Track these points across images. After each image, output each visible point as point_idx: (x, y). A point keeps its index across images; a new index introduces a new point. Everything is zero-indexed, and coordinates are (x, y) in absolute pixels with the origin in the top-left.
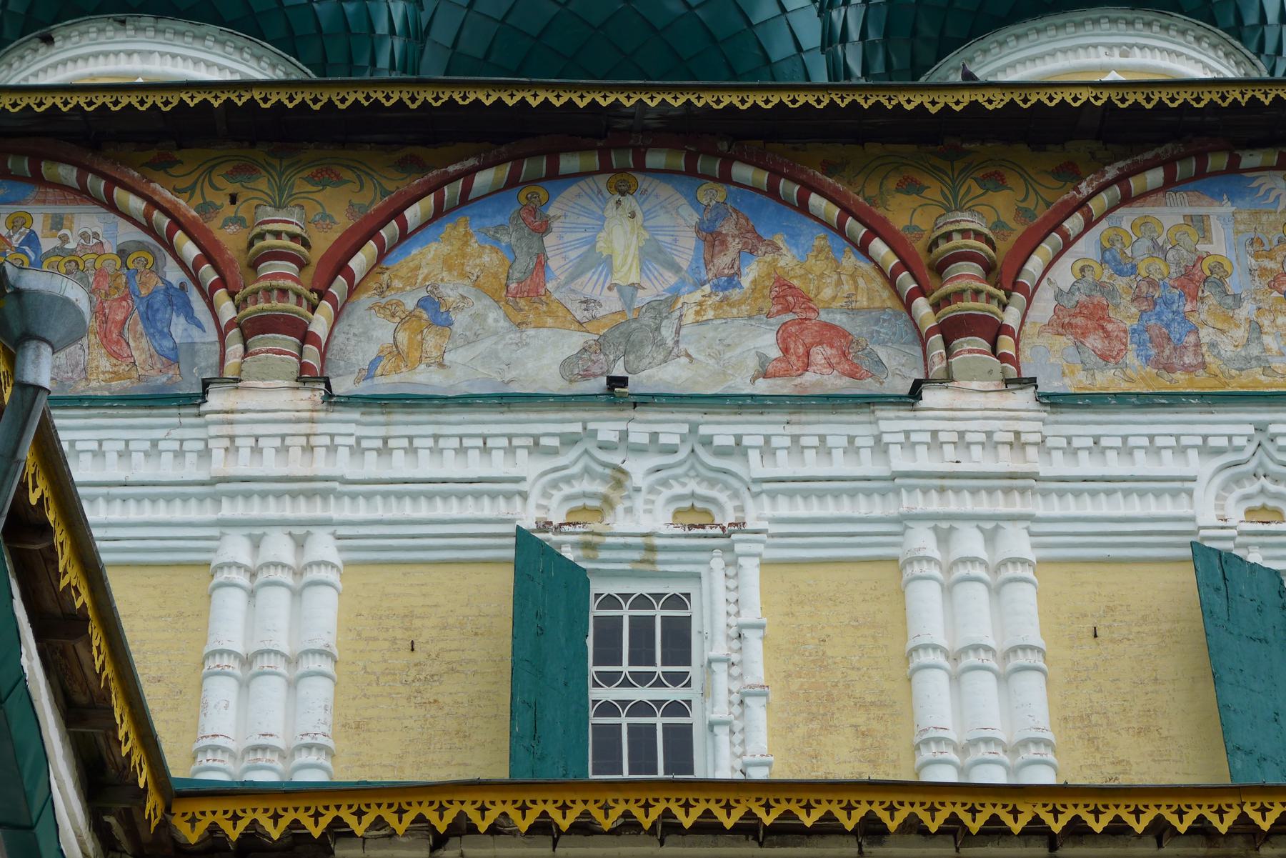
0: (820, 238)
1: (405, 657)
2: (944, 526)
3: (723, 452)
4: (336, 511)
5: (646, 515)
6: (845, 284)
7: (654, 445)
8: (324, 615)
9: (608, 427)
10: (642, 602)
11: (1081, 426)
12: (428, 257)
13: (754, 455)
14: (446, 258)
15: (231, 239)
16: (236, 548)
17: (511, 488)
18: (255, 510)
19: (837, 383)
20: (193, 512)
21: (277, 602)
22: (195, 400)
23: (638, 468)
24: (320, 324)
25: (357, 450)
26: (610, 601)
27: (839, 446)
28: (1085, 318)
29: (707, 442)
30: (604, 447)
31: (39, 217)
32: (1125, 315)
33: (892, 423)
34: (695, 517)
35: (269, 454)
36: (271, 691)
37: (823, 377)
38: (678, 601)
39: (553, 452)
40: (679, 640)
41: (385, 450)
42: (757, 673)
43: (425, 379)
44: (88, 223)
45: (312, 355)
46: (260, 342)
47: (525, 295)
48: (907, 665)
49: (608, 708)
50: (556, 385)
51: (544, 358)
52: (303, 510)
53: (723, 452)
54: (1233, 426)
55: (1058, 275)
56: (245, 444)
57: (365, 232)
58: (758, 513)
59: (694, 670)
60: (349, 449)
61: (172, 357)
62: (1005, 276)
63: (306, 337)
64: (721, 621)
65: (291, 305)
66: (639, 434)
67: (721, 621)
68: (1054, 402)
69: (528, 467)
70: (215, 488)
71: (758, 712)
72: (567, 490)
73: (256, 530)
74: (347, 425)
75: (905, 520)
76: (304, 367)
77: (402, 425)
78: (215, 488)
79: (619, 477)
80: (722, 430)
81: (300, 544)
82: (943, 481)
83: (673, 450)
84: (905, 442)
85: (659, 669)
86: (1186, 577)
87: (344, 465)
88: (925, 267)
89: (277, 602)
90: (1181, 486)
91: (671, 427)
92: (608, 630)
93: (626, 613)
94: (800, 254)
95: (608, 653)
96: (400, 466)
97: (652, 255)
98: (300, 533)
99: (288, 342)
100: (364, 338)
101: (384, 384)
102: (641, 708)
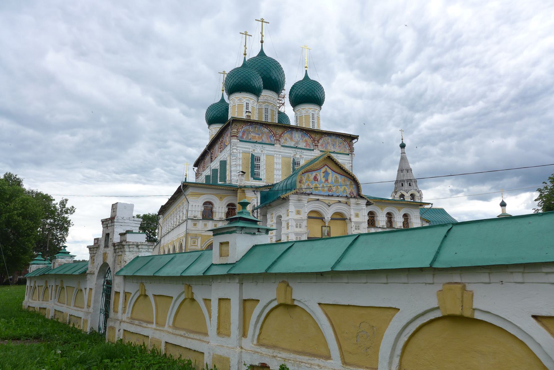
5: (298, 156)
6: (310, 141)
8: (280, 161)
12: (286, 135)
14: (287, 135)
16: (275, 155)
17: (291, 153)
19: (308, 148)
22: (274, 145)
28: (322, 145)
31: (263, 128)
32: (324, 145)
33: (312, 152)
37: (308, 148)
43: (286, 145)
44: (266, 129)
47: (291, 139)
50: (293, 146)
51: (292, 144)
55: (321, 141)
58: (304, 157)
60: (282, 149)
61: (271, 141)
62: (318, 142)
69: (292, 152)
70: (275, 151)
73: (277, 154)
74: (282, 148)
77: (286, 148)
78: (275, 151)
80: (303, 151)
88: (314, 140)
91: (300, 150)
94: (307, 138)
97: (299, 137)
101: (283, 145)
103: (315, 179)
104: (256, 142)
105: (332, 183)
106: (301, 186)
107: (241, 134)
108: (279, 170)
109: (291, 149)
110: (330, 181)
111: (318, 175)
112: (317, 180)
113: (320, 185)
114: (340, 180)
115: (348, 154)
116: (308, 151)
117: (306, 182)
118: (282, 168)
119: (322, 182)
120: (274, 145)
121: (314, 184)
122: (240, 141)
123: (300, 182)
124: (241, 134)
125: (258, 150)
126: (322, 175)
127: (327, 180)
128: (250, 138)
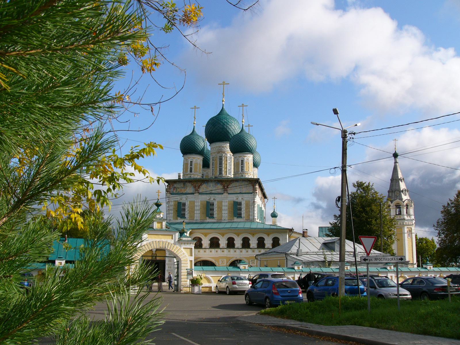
0: (220, 185)
2: (224, 200)
11: (230, 195)
15: (195, 185)
21: (198, 203)
23: (212, 197)
27: (220, 196)
33: (222, 195)
34: (214, 199)
44: (189, 184)
48: (222, 206)
54: (236, 195)
57: (200, 185)
68: (229, 194)
71: (216, 208)
82: (224, 198)
84: (223, 196)
86: (233, 202)
87: (200, 197)
89: (198, 203)
90: (234, 198)
98: (198, 200)
100: (201, 190)
107: (172, 190)
108: (197, 210)
109: (233, 195)
115: (252, 193)
116: (220, 195)
118: (201, 208)
122: (171, 194)
124: (172, 190)
125: (183, 199)
128: (178, 191)
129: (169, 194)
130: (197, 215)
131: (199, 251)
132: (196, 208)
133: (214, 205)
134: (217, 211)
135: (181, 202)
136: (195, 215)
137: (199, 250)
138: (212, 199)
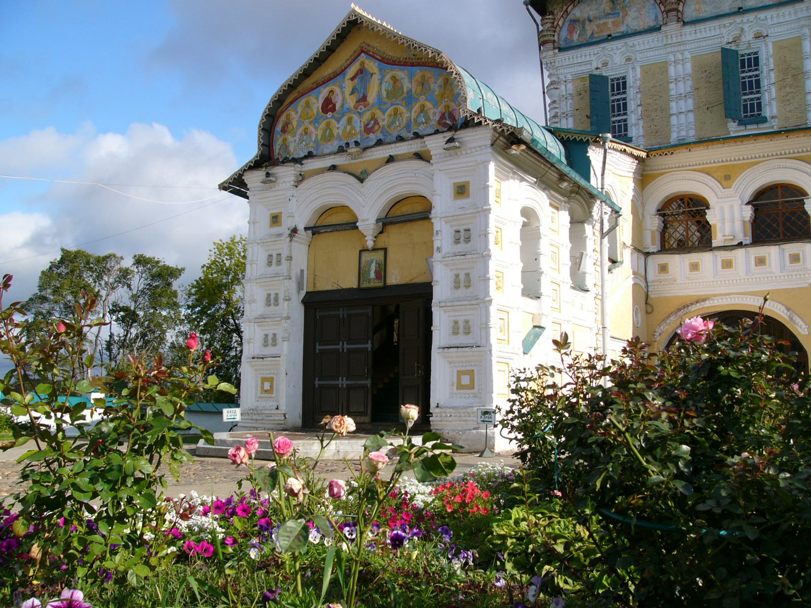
1: (704, 75)
3: (763, 20)
4: (688, 47)
7: (748, 21)
9: (738, 19)
10: (749, 55)
13: (769, 20)
18: (673, 49)
20: (662, 52)
22: (659, 29)
23: (746, 27)
24: (680, 8)
25: (690, 34)
26: (743, 56)
29: (759, 18)
30: (738, 24)
34: (758, 36)
35: (674, 38)
36: (681, 84)
38: (756, 53)
39: (728, 27)
40: (757, 60)
41: (696, 33)
42: (772, 66)
45: (680, 16)
46: (670, 14)
49: (744, 78)
52: (682, 48)
53: (763, 20)
56: (669, 37)
59: (760, 67)
63: (678, 11)
64: (764, 56)
65: (674, 6)
66: (745, 20)
67: (764, 56)
72: (732, 34)
74: (688, 29)
75: (802, 26)
76: (679, 18)
79: (742, 29)
81: (682, 54)
83: (752, 22)
85: (747, 80)
87: (689, 38)
91: (751, 17)
92: (743, 61)
93: (746, 57)
95: (743, 66)
96: (699, 36)
99: (675, 13)
102: (750, 77)
103: (328, 106)
104: (610, 38)
105: (380, 102)
106: (285, 140)
107: (564, 33)
108: (680, 97)
110: (372, 98)
111: (337, 89)
112: (333, 109)
113: (338, 121)
114: (406, 85)
117: (298, 126)
119: (349, 110)
120: (656, 29)
121: (323, 125)
123: (284, 131)
124: (564, 33)
126: (348, 85)
127: (364, 99)
128: (589, 33)
129: (551, 53)
130: (682, 117)
131: (695, 267)
132: (674, 89)
133: (762, 62)
134: (779, 89)
135: (606, 78)
136: (674, 120)
137: (694, 257)
138: (748, 36)
